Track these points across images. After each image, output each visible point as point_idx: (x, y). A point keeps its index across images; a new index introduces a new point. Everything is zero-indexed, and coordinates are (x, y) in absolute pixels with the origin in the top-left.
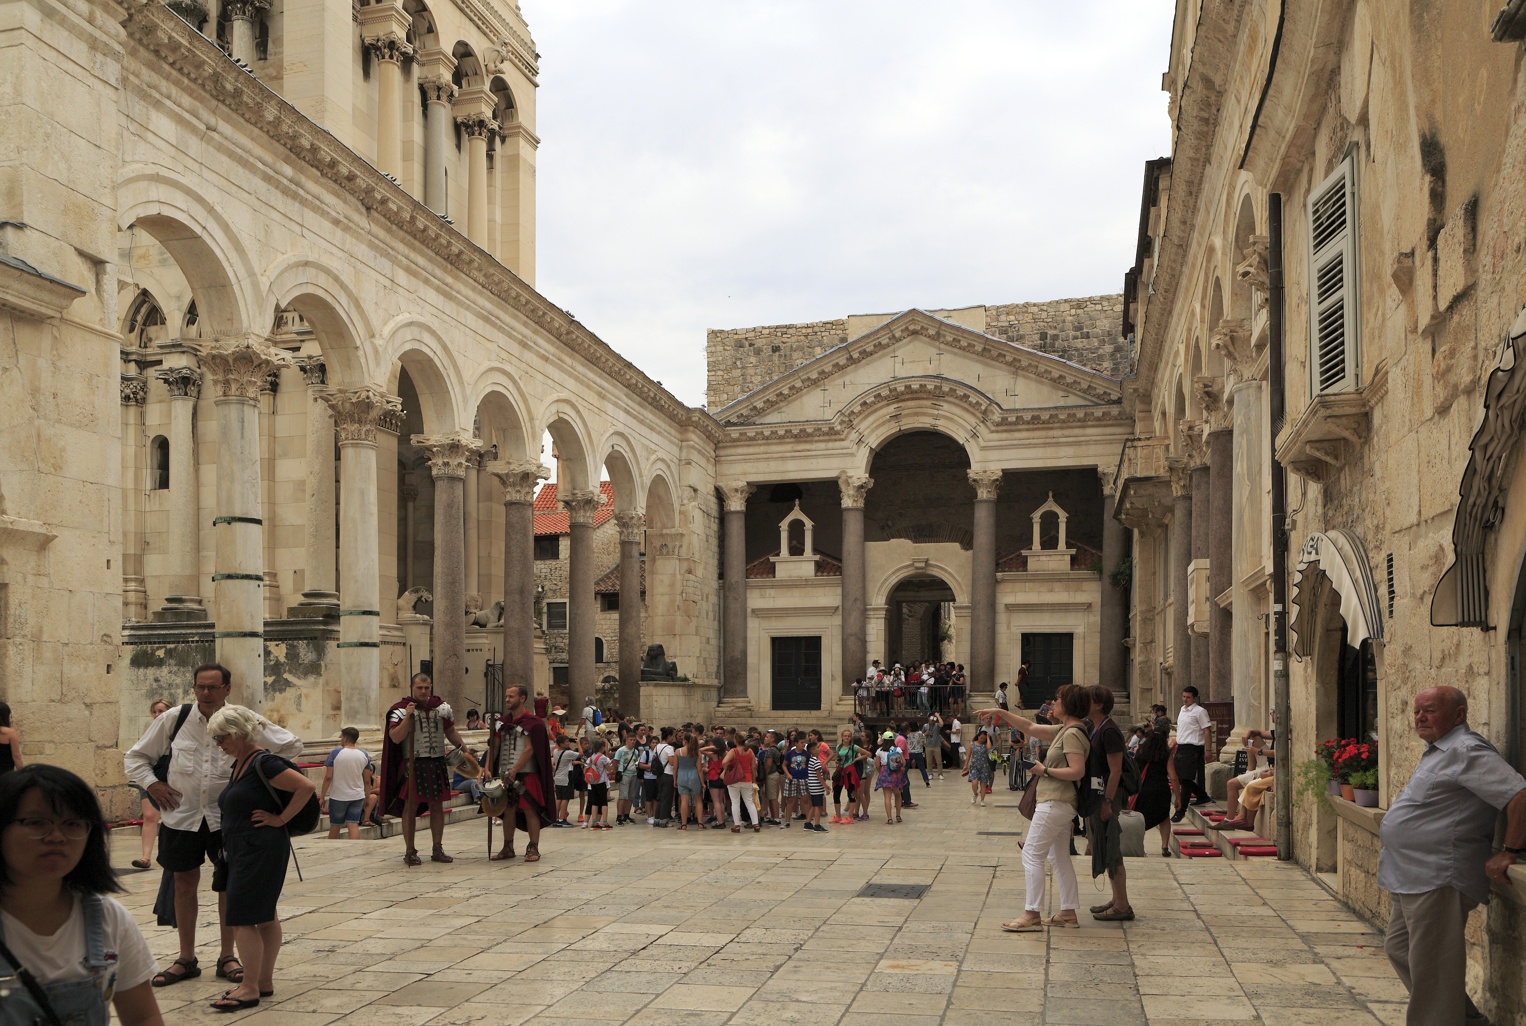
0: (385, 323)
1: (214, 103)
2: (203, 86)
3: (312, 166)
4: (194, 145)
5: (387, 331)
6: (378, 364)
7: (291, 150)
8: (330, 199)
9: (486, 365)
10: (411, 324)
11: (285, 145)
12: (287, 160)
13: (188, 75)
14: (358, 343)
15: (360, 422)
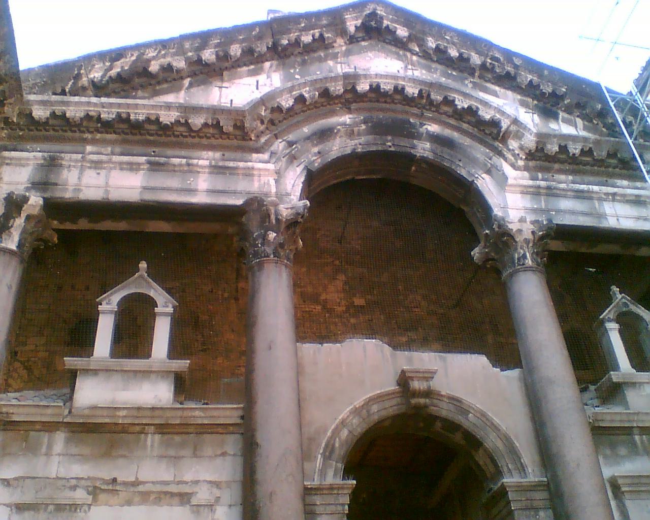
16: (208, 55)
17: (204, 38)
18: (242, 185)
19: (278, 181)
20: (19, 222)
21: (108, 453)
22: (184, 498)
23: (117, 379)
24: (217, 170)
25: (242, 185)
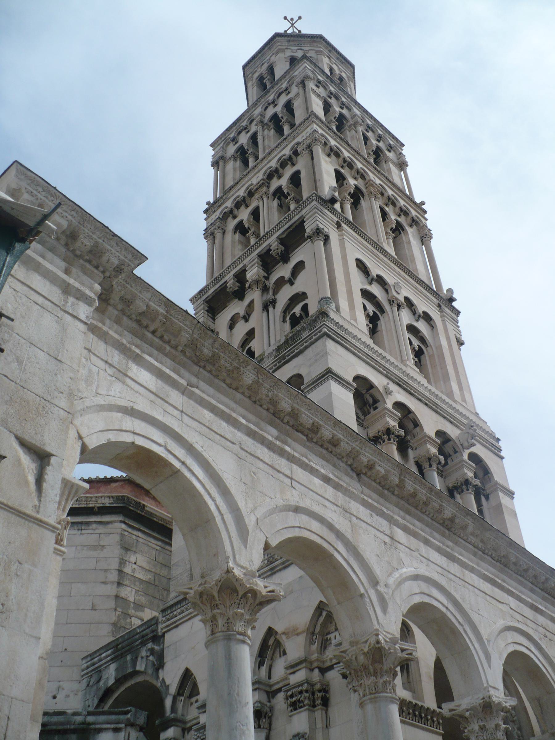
0: (390, 575)
1: (196, 368)
2: (183, 352)
3: (297, 431)
4: (175, 397)
5: (391, 581)
6: (385, 609)
7: (274, 414)
8: (317, 463)
9: (501, 623)
10: (416, 577)
11: (268, 410)
12: (271, 424)
13: (169, 342)
14: (362, 591)
15: (375, 674)
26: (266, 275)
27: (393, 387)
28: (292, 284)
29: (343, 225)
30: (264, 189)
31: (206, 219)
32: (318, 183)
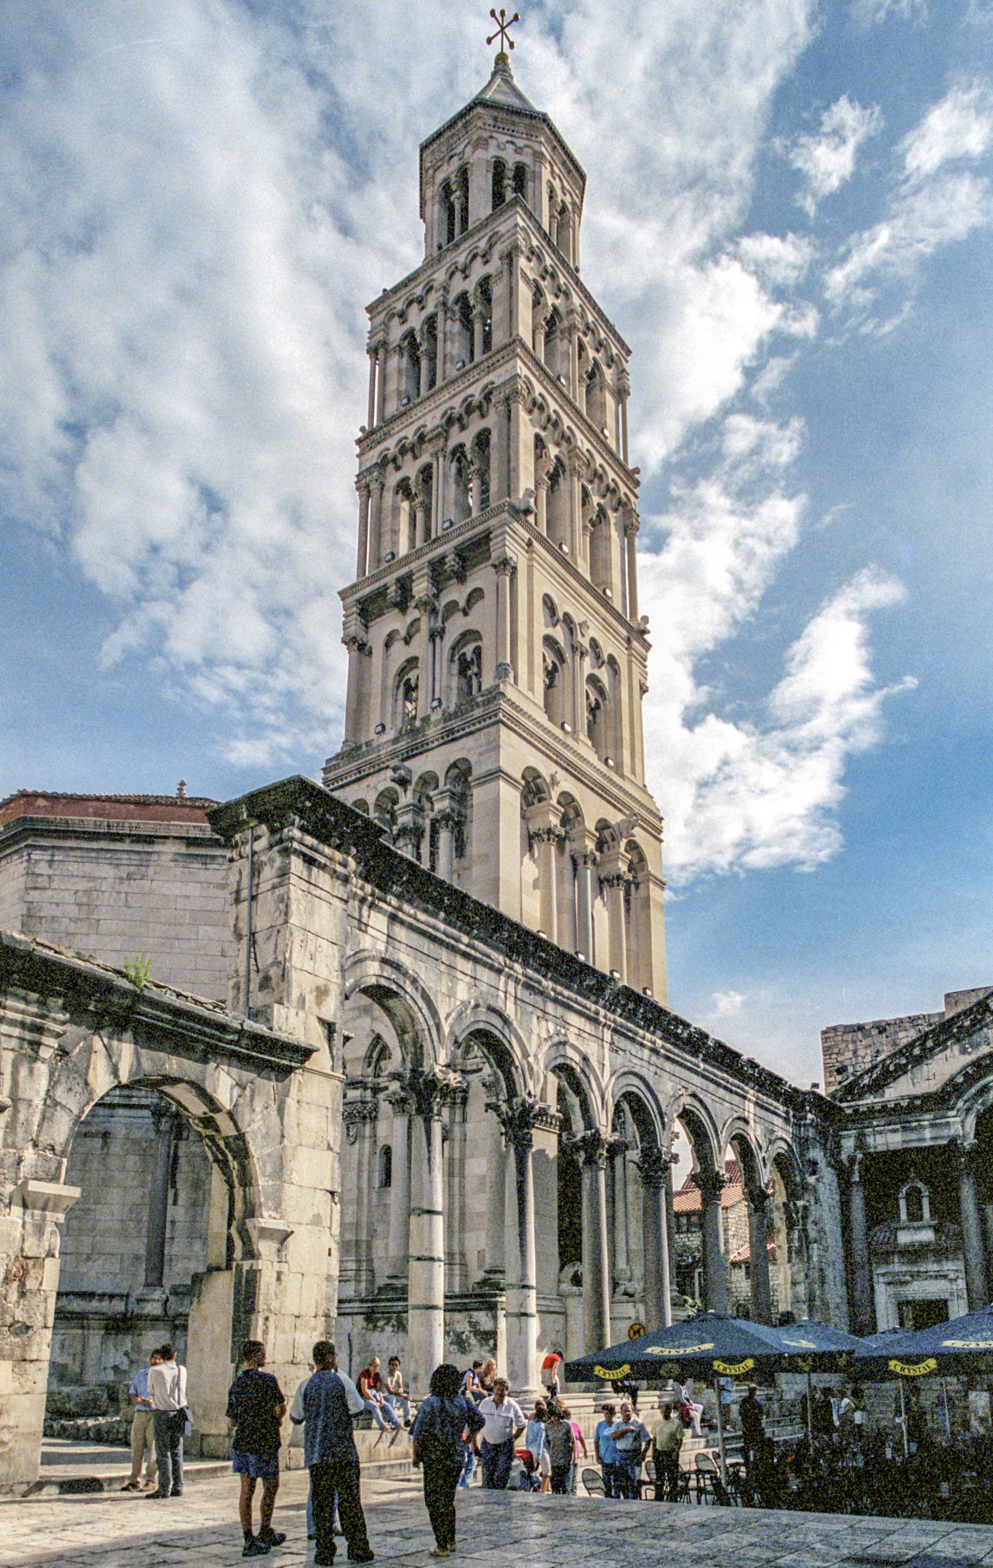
16: (917, 1051)
17: (911, 1045)
18: (945, 1132)
19: (961, 1126)
20: (856, 1167)
21: (915, 1262)
22: (945, 1277)
23: (912, 1232)
24: (932, 1126)
25: (945, 1132)
26: (435, 591)
27: (561, 775)
28: (466, 614)
29: (535, 544)
30: (441, 443)
31: (359, 456)
32: (513, 474)
